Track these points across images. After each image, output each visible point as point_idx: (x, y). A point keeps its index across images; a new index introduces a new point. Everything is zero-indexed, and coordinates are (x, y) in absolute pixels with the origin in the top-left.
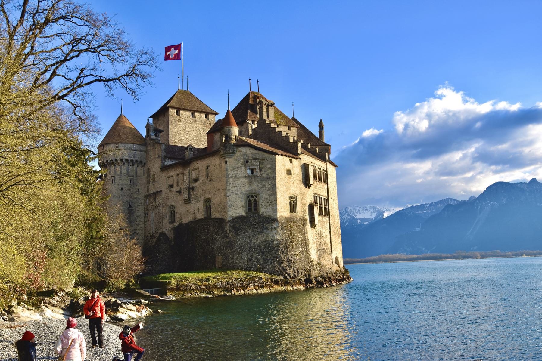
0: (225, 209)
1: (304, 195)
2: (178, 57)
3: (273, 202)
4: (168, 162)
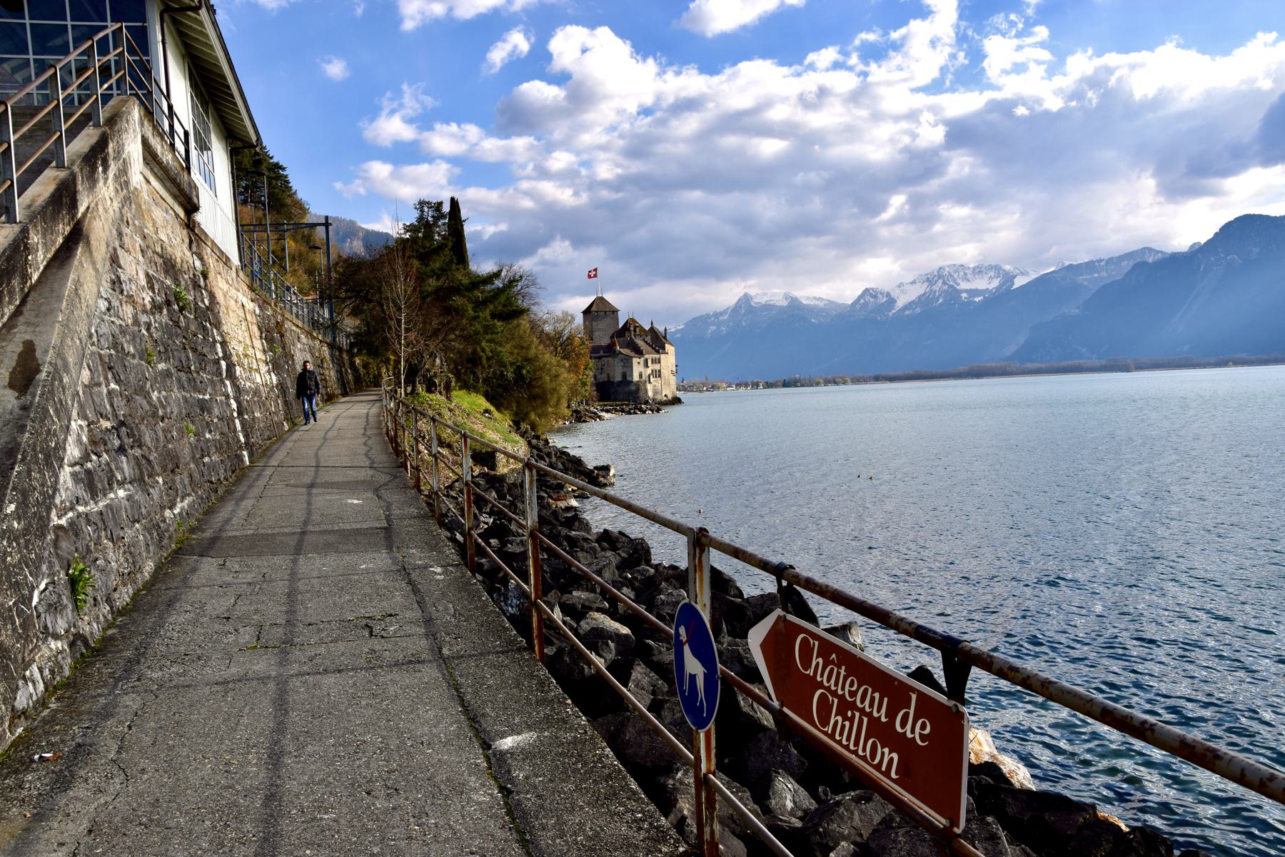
0: (614, 378)
1: (646, 372)
2: (595, 276)
3: (632, 375)
4: (593, 355)
